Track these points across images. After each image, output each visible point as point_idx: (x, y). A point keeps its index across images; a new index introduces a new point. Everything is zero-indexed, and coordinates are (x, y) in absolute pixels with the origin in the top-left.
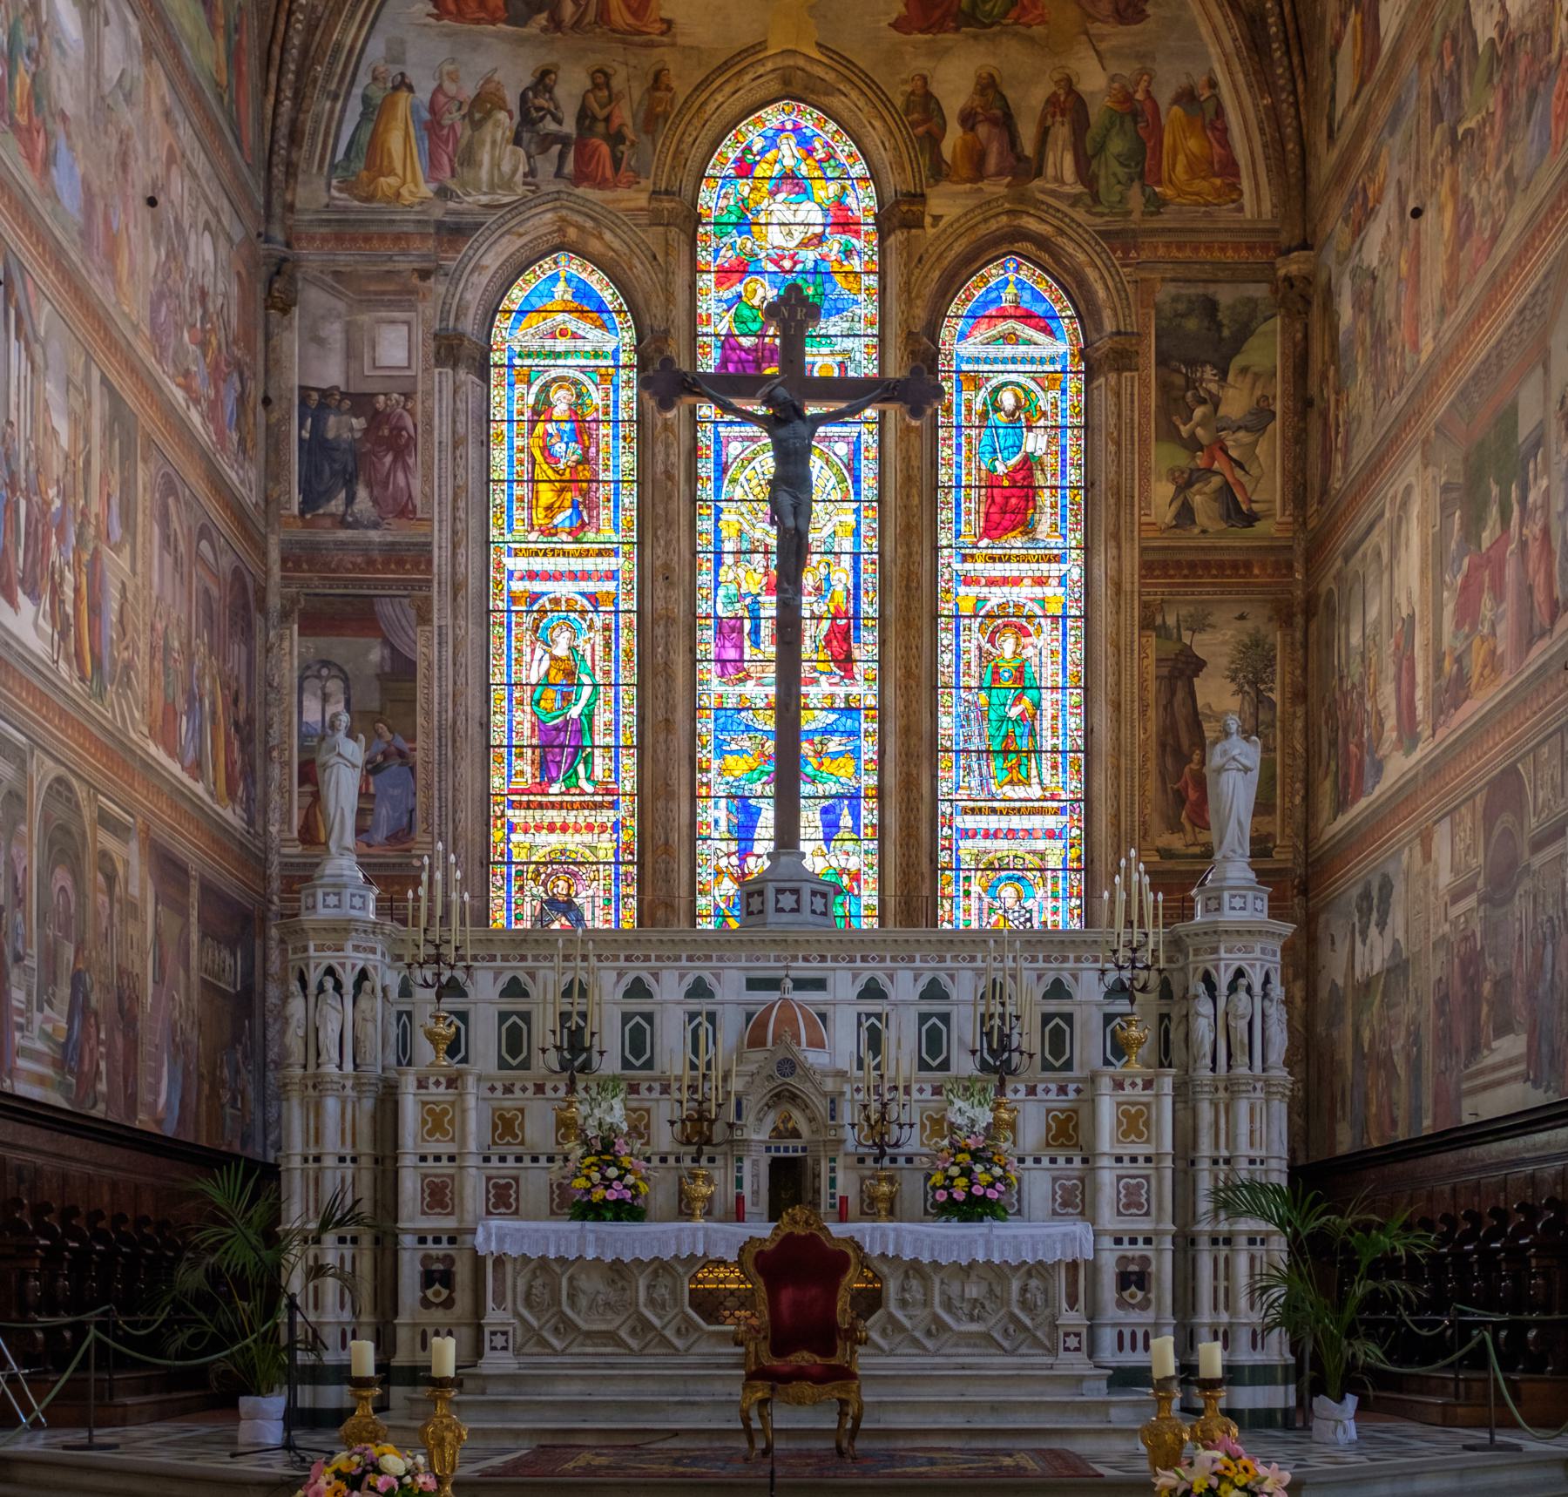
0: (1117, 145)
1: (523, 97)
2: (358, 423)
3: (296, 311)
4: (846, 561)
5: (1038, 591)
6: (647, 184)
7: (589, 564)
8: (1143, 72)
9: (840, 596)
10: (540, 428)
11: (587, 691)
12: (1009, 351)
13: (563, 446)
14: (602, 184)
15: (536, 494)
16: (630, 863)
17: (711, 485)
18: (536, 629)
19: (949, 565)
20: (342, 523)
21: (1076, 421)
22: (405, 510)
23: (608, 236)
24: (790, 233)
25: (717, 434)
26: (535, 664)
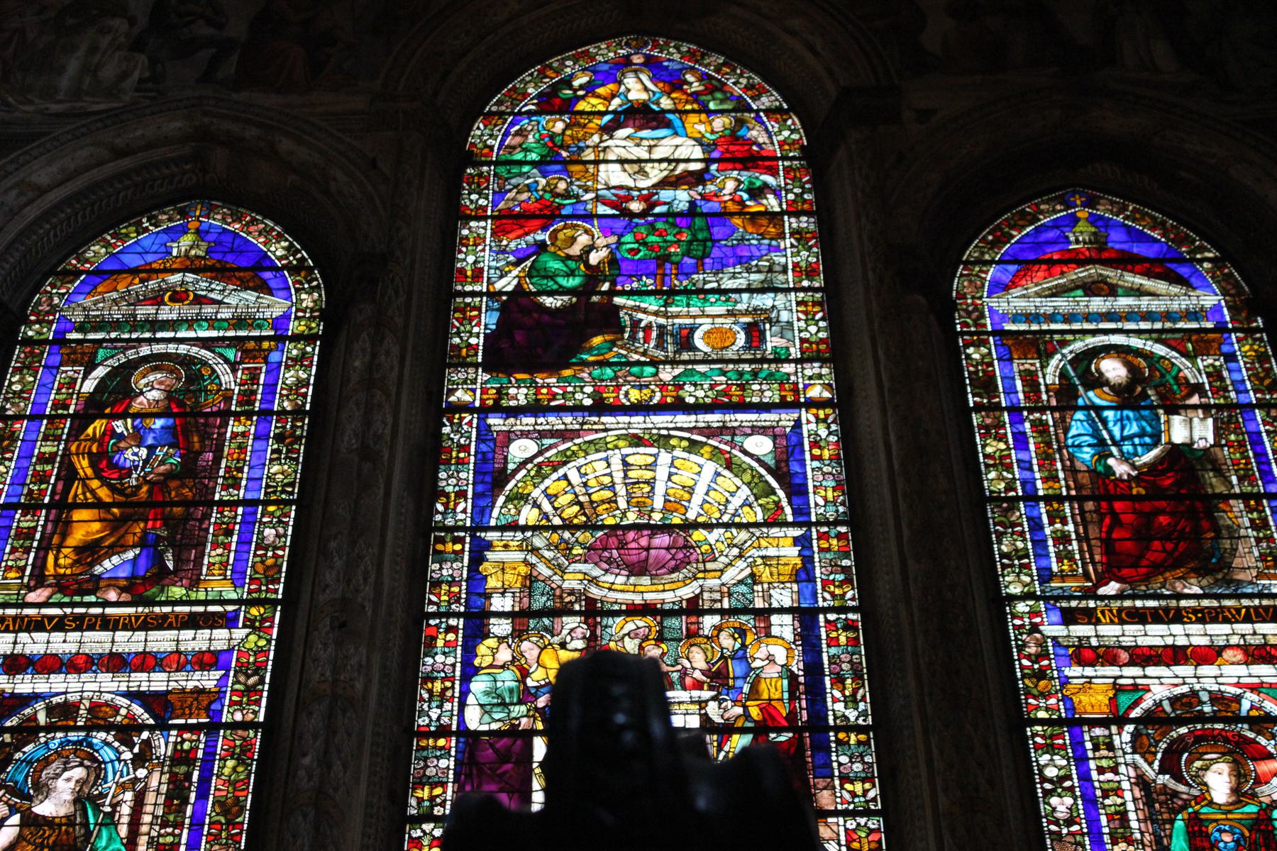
4: (784, 626)
9: (774, 688)
10: (98, 426)
12: (1098, 304)
13: (143, 452)
15: (63, 526)
17: (465, 505)
19: (1035, 628)
24: (642, 172)
25: (484, 432)
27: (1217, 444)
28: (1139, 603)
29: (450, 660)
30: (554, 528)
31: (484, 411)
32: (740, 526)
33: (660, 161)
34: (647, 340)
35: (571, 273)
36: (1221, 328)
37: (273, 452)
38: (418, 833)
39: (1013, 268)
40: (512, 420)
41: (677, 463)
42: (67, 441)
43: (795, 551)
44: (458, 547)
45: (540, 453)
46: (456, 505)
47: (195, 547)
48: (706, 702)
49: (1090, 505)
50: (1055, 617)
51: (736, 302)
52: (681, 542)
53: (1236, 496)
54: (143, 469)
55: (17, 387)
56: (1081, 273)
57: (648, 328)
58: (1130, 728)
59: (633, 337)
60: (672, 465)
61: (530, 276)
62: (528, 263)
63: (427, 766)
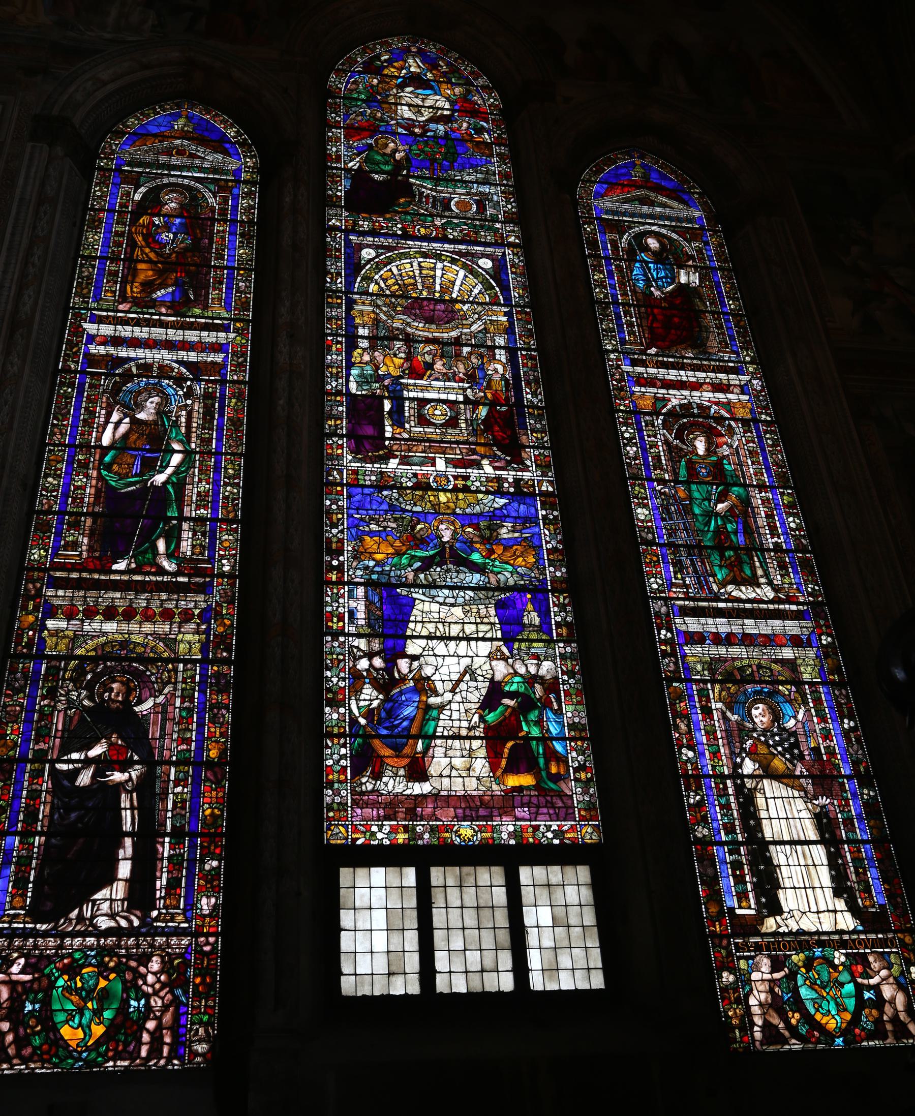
4: (501, 355)
5: (721, 396)
7: (192, 336)
9: (499, 385)
10: (144, 220)
11: (176, 459)
12: (645, 209)
13: (171, 236)
16: (226, 661)
19: (618, 367)
24: (419, 112)
25: (348, 242)
26: (110, 427)
27: (700, 285)
28: (665, 359)
29: (339, 358)
30: (387, 296)
31: (347, 232)
32: (478, 304)
33: (429, 107)
34: (427, 203)
35: (386, 163)
36: (702, 228)
37: (240, 242)
38: (331, 442)
39: (605, 186)
40: (361, 238)
41: (446, 268)
42: (129, 226)
43: (505, 319)
44: (339, 301)
45: (377, 257)
46: (337, 279)
47: (204, 288)
48: (466, 389)
49: (643, 310)
50: (628, 362)
51: (471, 188)
52: (450, 309)
53: (708, 312)
54: (172, 244)
55: (99, 193)
56: (638, 193)
57: (427, 196)
58: (662, 417)
59: (420, 201)
60: (443, 269)
61: (365, 161)
62: (364, 155)
63: (332, 410)
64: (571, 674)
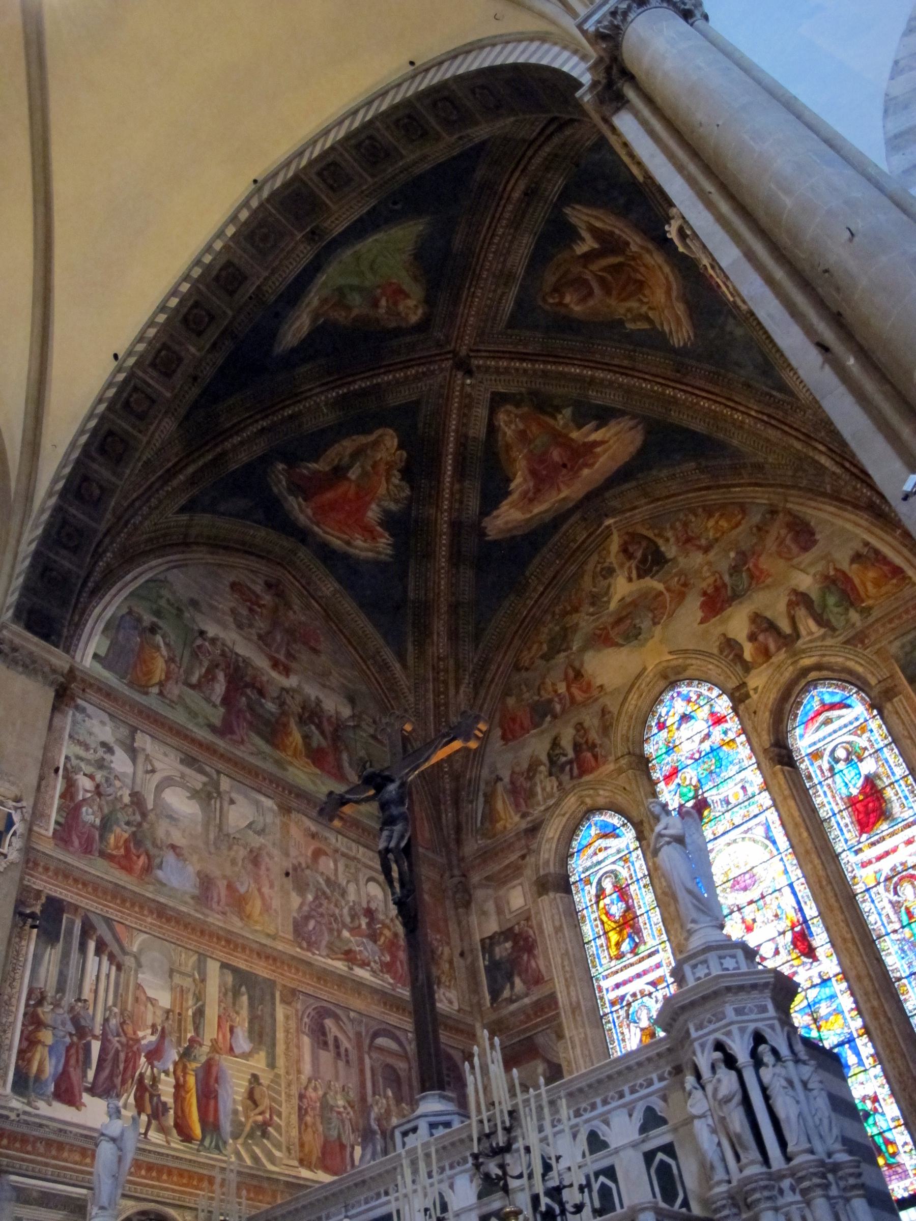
0: (831, 600)
1: (549, 755)
2: (508, 945)
3: (473, 905)
4: (787, 891)
6: (612, 758)
8: (828, 562)
10: (601, 904)
14: (591, 771)
15: (608, 939)
18: (628, 1015)
20: (511, 1001)
21: (886, 742)
22: (537, 980)
23: (601, 792)
56: (821, 718)
64: (882, 1086)
